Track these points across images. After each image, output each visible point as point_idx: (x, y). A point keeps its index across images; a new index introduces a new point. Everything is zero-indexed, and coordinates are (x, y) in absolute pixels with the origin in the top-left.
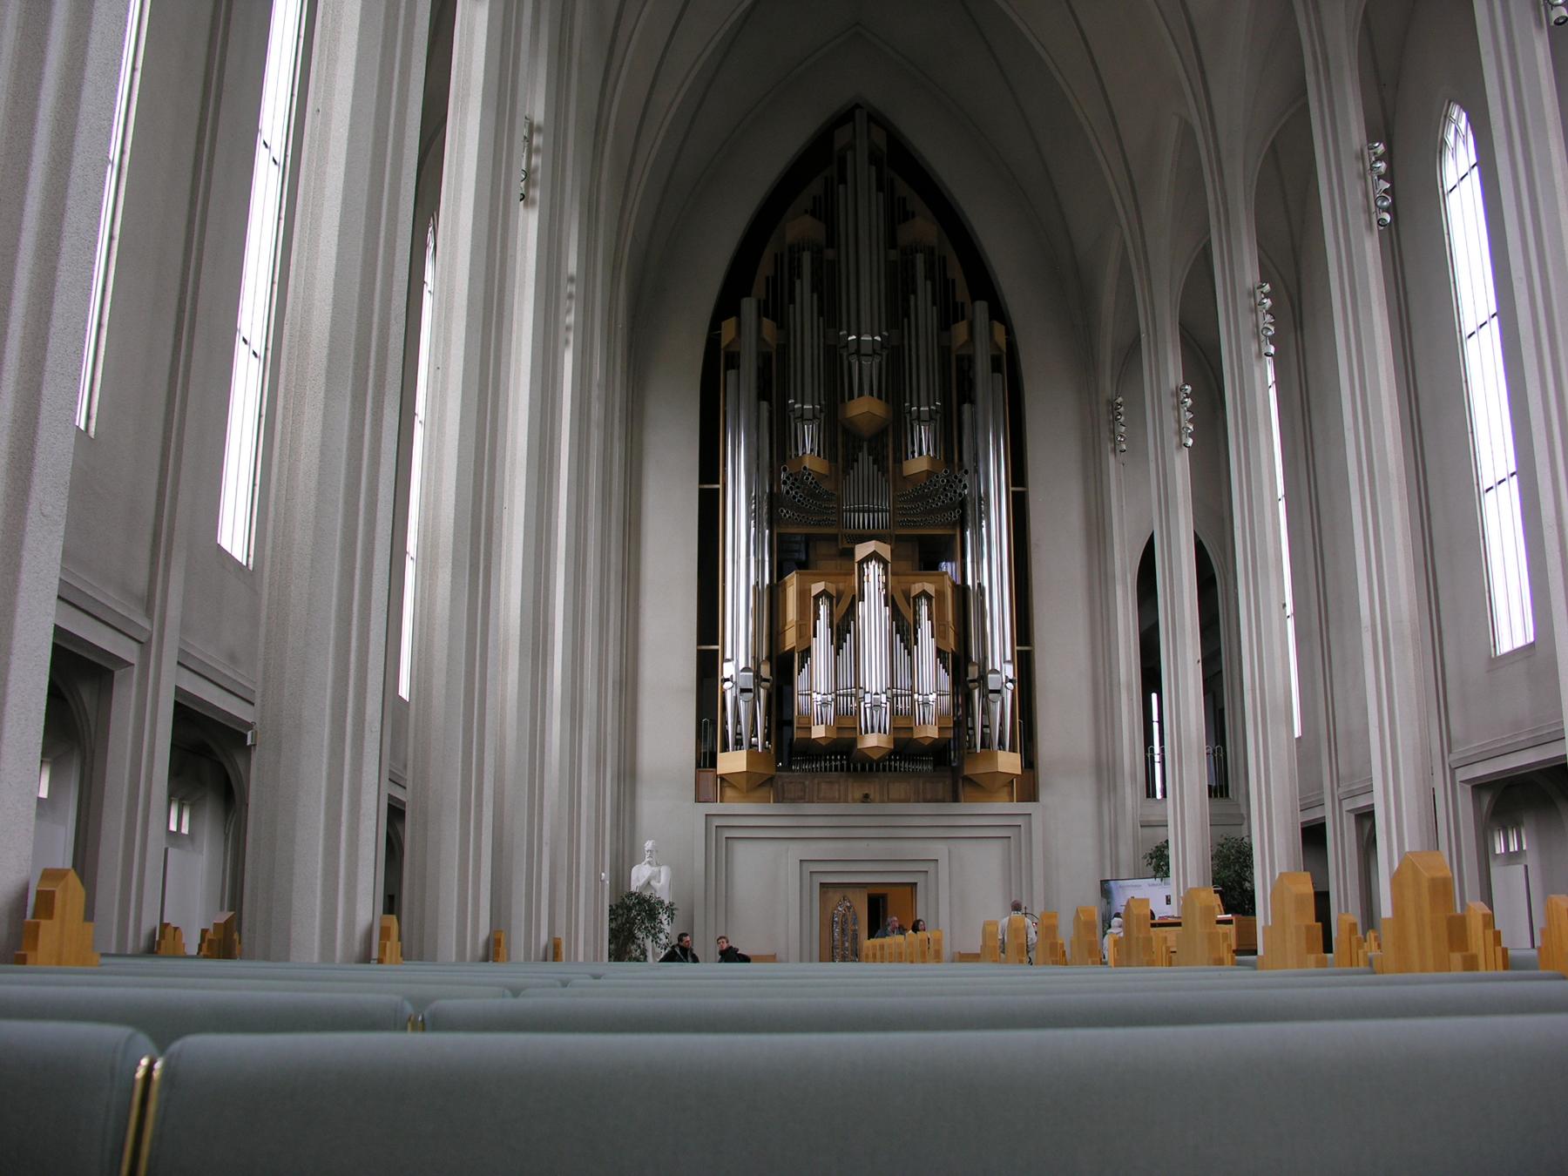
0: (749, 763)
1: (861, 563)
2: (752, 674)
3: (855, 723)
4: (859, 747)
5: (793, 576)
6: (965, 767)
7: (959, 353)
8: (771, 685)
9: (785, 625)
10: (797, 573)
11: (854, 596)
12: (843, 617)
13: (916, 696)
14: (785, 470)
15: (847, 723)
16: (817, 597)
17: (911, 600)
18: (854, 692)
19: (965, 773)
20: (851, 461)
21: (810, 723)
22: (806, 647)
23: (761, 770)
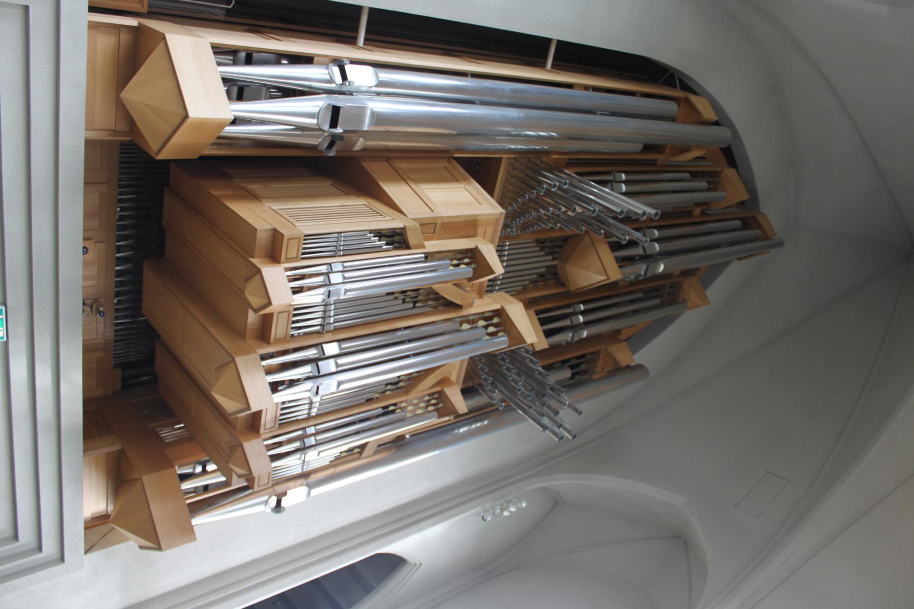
0: (202, 124)
1: (500, 313)
2: (366, 128)
3: (279, 341)
4: (238, 360)
5: (494, 208)
6: (153, 475)
7: (602, 356)
8: (320, 151)
9: (413, 181)
10: (501, 213)
11: (459, 307)
12: (437, 293)
13: (311, 430)
14: (656, 214)
15: (278, 329)
16: (473, 255)
17: (439, 389)
18: (327, 328)
19: (145, 478)
20: (541, 243)
21: (288, 260)
22: (412, 241)
23: (178, 139)
